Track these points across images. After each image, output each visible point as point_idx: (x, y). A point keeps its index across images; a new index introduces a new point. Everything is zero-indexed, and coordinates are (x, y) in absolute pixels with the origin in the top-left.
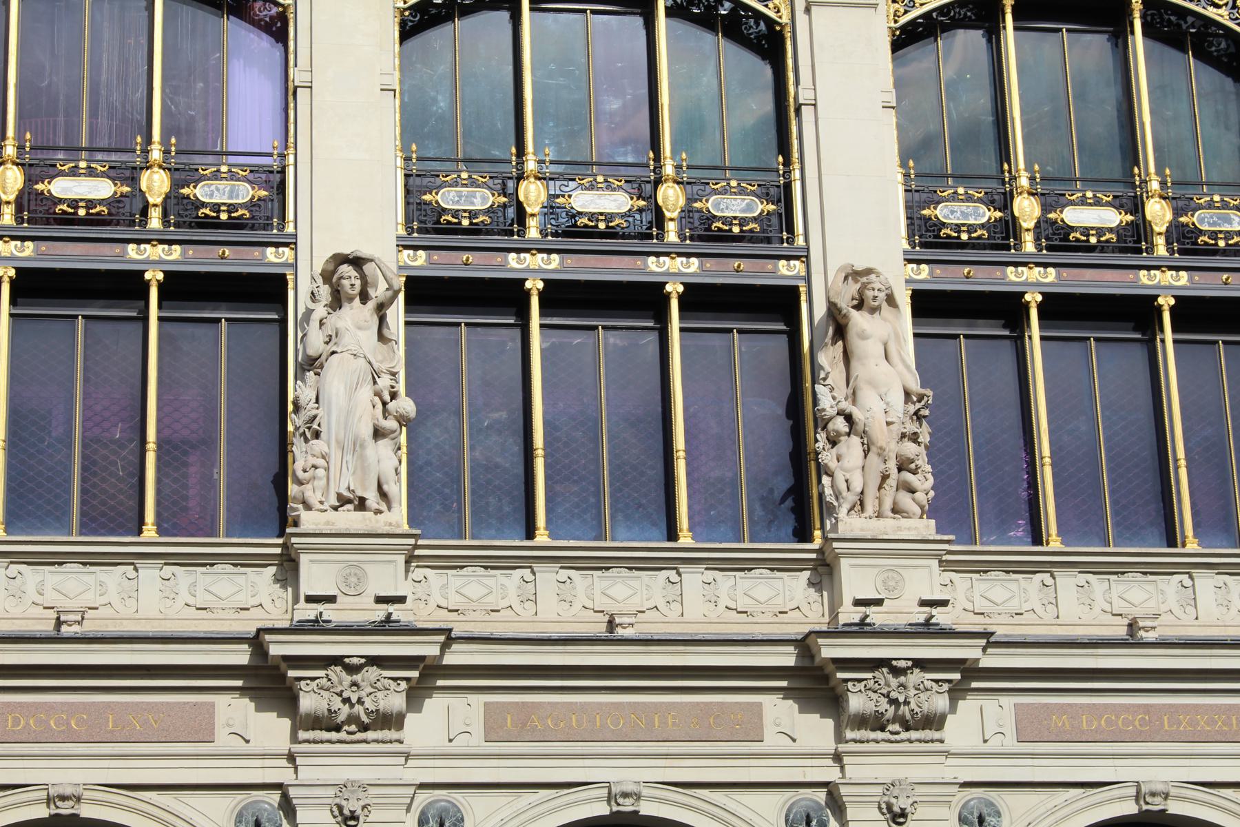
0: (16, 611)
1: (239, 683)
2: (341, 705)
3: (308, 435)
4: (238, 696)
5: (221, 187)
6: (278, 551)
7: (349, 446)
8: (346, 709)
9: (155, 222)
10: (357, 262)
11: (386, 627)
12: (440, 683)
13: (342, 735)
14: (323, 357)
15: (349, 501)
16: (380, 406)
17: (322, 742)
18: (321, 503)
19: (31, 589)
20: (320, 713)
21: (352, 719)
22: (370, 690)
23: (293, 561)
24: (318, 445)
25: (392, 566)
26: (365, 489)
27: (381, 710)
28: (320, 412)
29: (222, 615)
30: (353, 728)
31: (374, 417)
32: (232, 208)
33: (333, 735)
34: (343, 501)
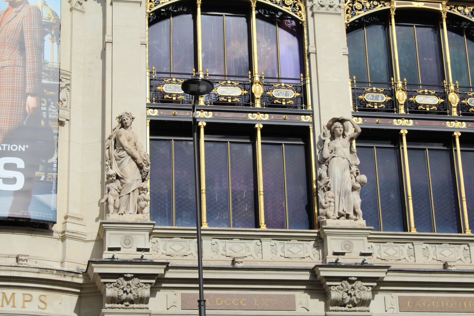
0: (216, 257)
1: (304, 287)
2: (347, 296)
3: (325, 189)
4: (303, 292)
5: (282, 92)
6: (316, 235)
7: (343, 194)
8: (349, 298)
9: (258, 105)
10: (342, 121)
11: (363, 266)
12: (381, 288)
13: (346, 308)
14: (329, 159)
15: (343, 215)
16: (354, 178)
17: (338, 311)
18: (333, 216)
19: (221, 249)
20: (338, 299)
21: (351, 302)
22: (358, 290)
23: (321, 239)
24: (330, 193)
25: (362, 241)
26: (349, 211)
27: (362, 299)
28: (330, 180)
29: (295, 260)
30: (351, 305)
31: (352, 182)
32: (287, 100)
33: (343, 308)
34: (340, 215)
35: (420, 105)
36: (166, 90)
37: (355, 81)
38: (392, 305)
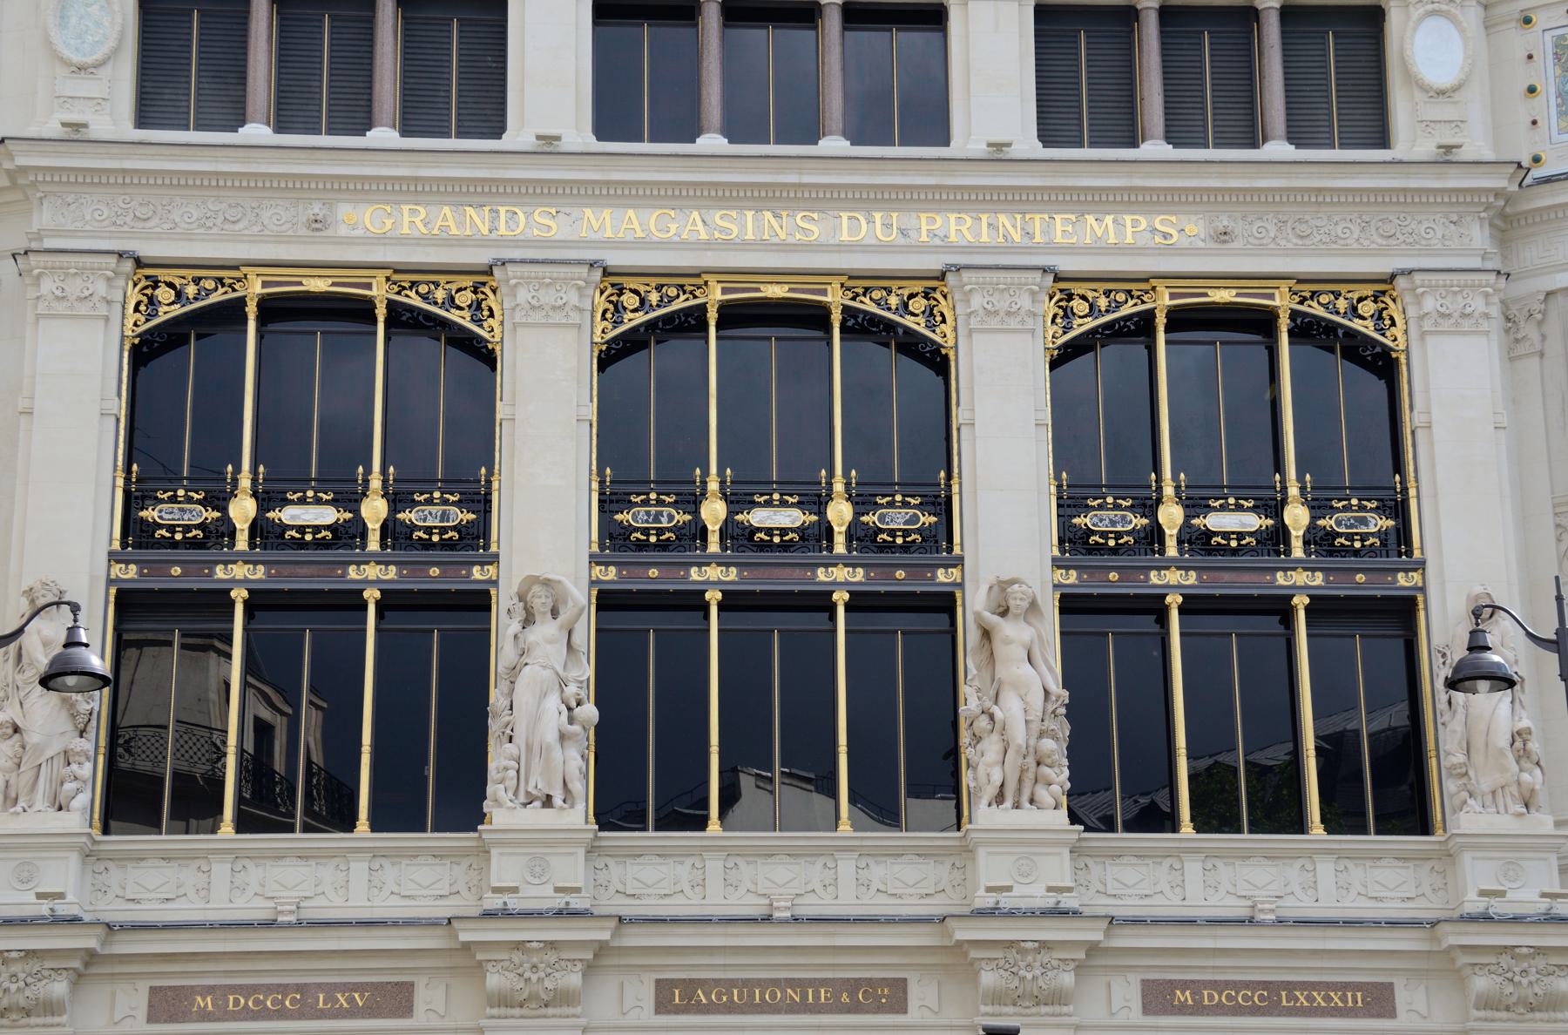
5: (434, 512)
35: (1216, 534)
36: (161, 517)
37: (854, 481)
38: (639, 1000)
